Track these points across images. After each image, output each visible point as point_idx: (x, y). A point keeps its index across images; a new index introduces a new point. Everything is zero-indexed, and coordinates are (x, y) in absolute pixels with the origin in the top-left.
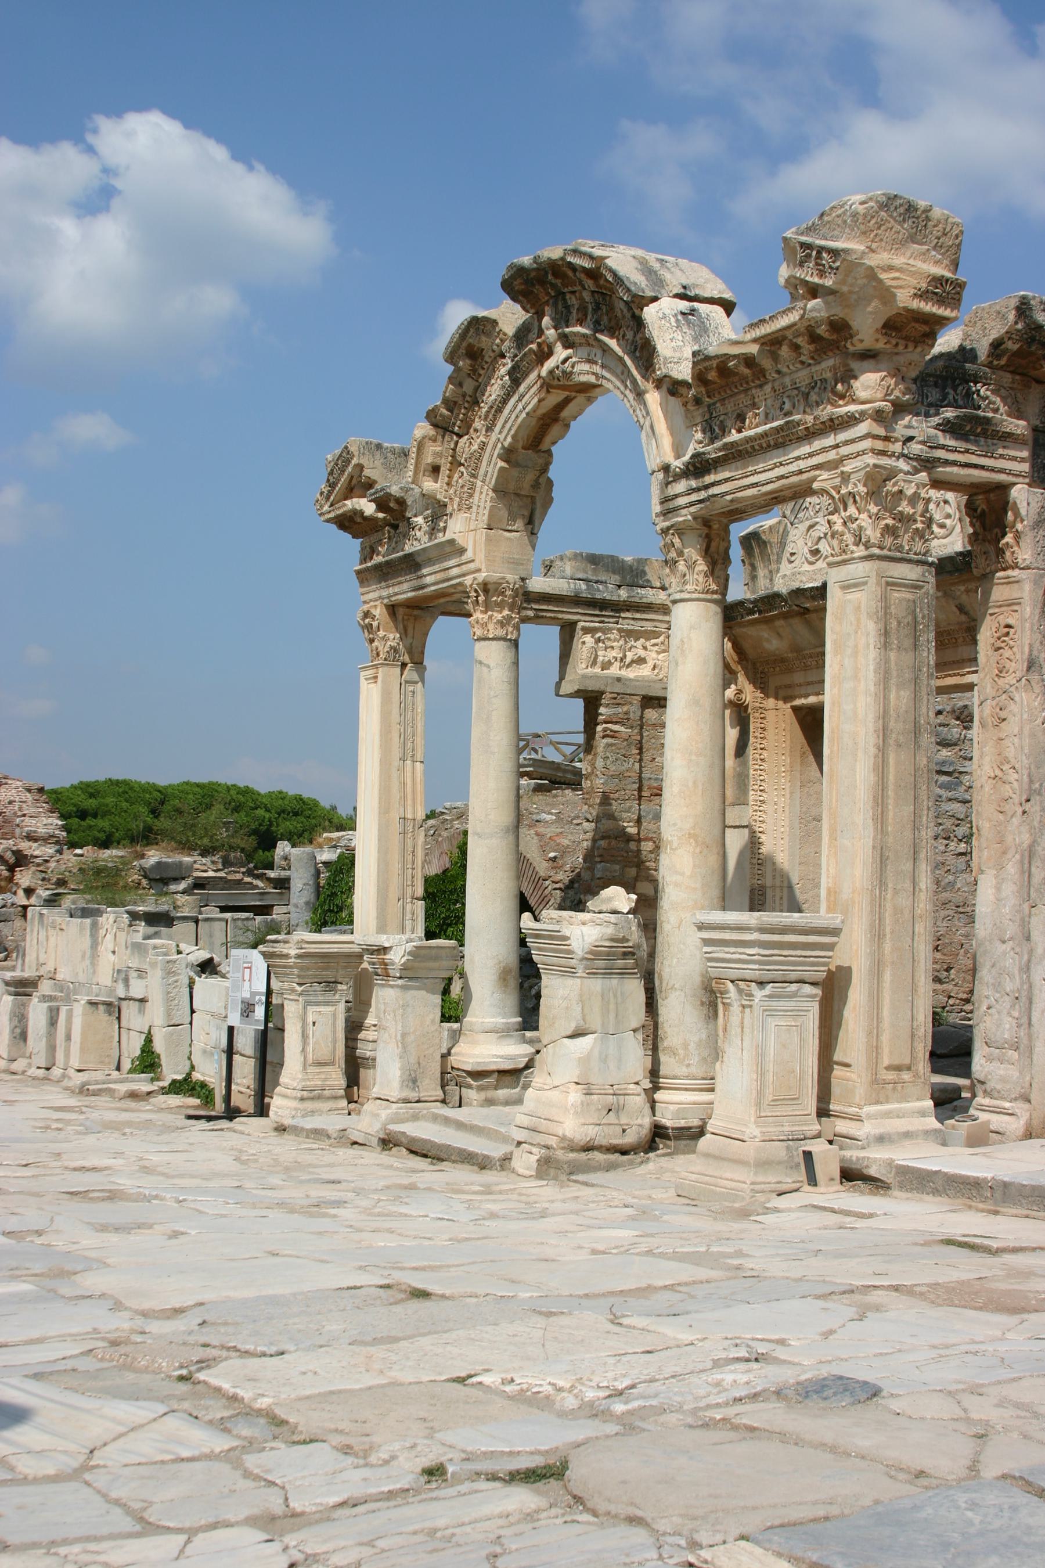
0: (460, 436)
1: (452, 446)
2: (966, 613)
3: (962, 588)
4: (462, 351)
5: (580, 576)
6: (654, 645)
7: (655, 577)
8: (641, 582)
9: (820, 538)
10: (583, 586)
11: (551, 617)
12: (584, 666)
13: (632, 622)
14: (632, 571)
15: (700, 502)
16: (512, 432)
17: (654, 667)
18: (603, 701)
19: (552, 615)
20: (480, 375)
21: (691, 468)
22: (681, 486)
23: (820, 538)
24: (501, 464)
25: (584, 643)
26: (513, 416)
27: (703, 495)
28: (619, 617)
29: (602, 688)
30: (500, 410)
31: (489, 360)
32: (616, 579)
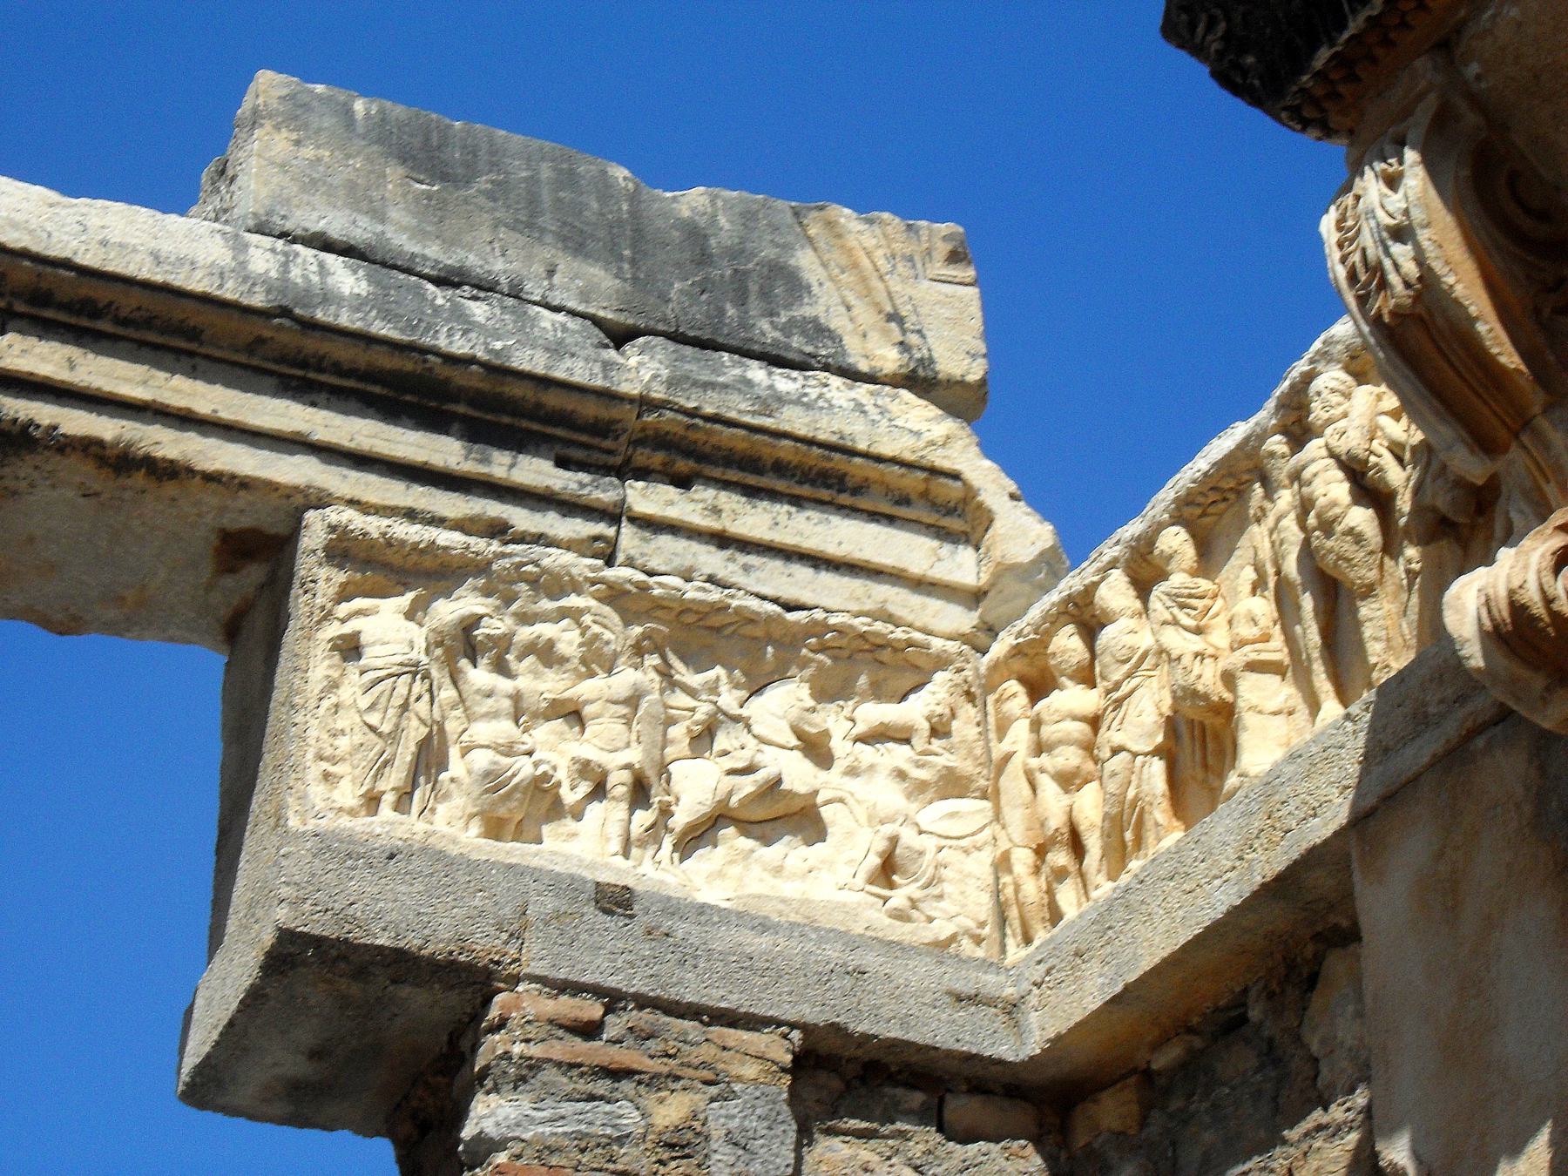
5: (336, 224)
6: (878, 736)
7: (865, 315)
8: (767, 331)
10: (347, 279)
11: (89, 447)
12: (348, 794)
13: (711, 560)
14: (704, 258)
17: (888, 869)
18: (492, 1046)
19: (106, 428)
25: (350, 649)
28: (613, 515)
29: (485, 944)
32: (597, 284)
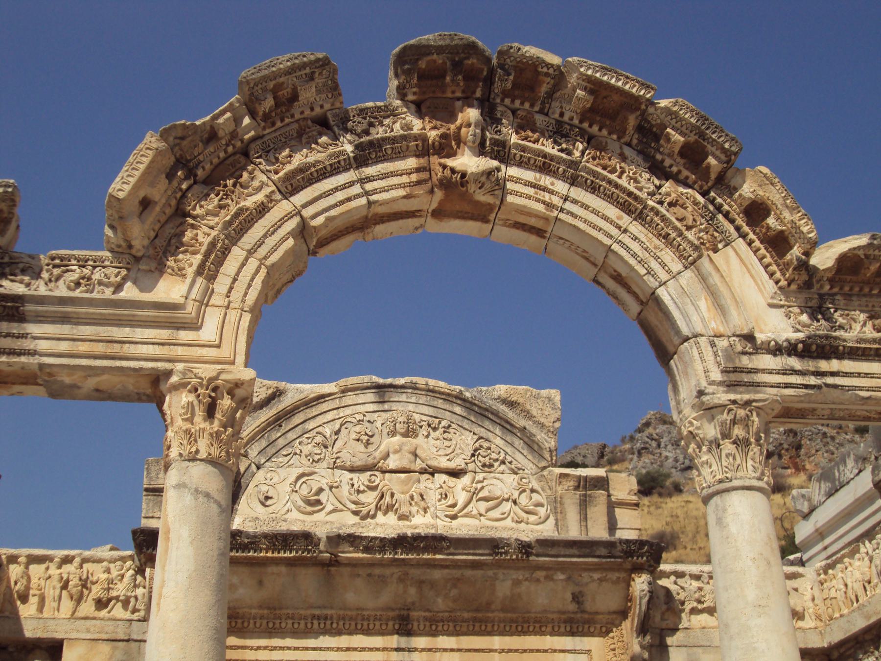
0: (195, 183)
1: (184, 186)
2: (578, 603)
3: (596, 576)
4: (271, 85)
9: (321, 490)
15: (806, 386)
16: (333, 213)
20: (273, 124)
21: (800, 346)
22: (767, 361)
23: (321, 490)
24: (291, 242)
26: (340, 196)
27: (812, 380)
30: (311, 181)
31: (297, 116)
